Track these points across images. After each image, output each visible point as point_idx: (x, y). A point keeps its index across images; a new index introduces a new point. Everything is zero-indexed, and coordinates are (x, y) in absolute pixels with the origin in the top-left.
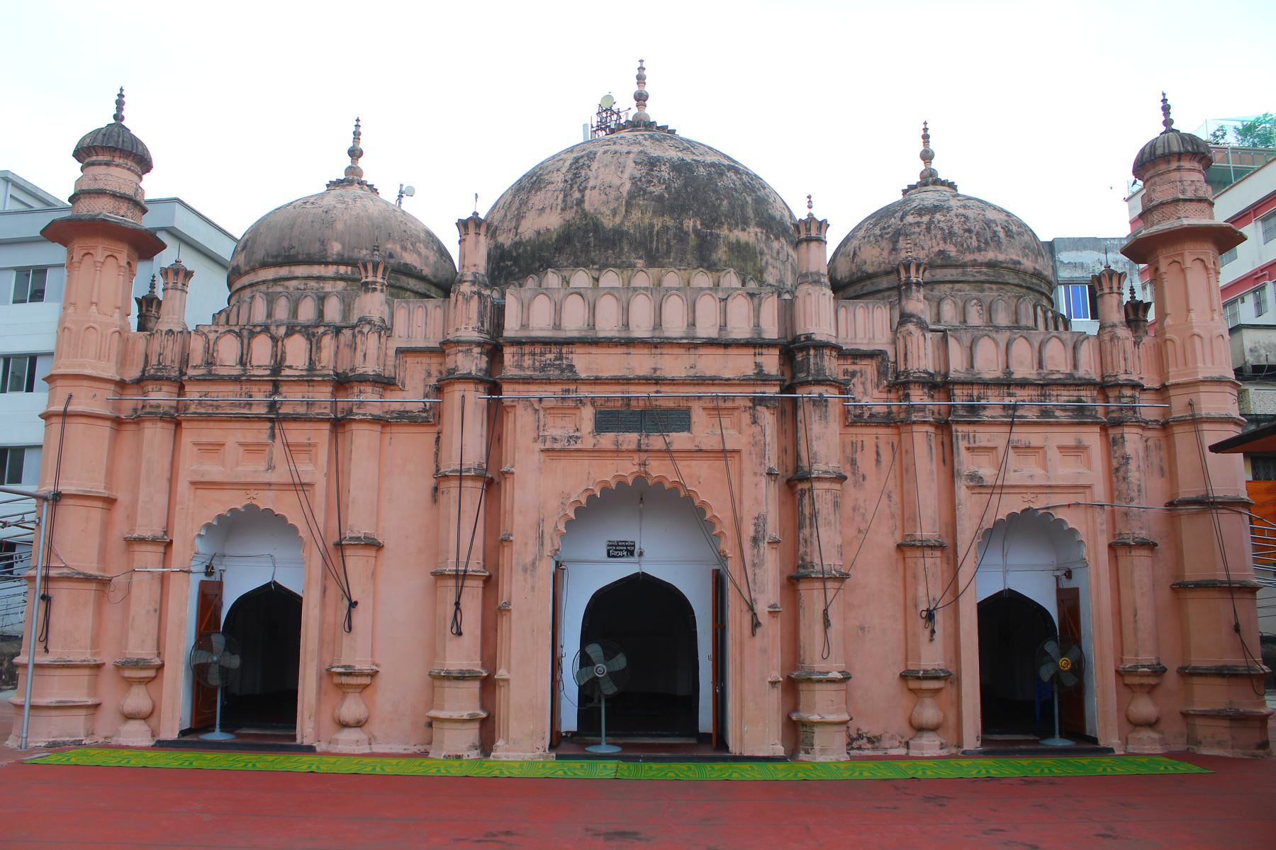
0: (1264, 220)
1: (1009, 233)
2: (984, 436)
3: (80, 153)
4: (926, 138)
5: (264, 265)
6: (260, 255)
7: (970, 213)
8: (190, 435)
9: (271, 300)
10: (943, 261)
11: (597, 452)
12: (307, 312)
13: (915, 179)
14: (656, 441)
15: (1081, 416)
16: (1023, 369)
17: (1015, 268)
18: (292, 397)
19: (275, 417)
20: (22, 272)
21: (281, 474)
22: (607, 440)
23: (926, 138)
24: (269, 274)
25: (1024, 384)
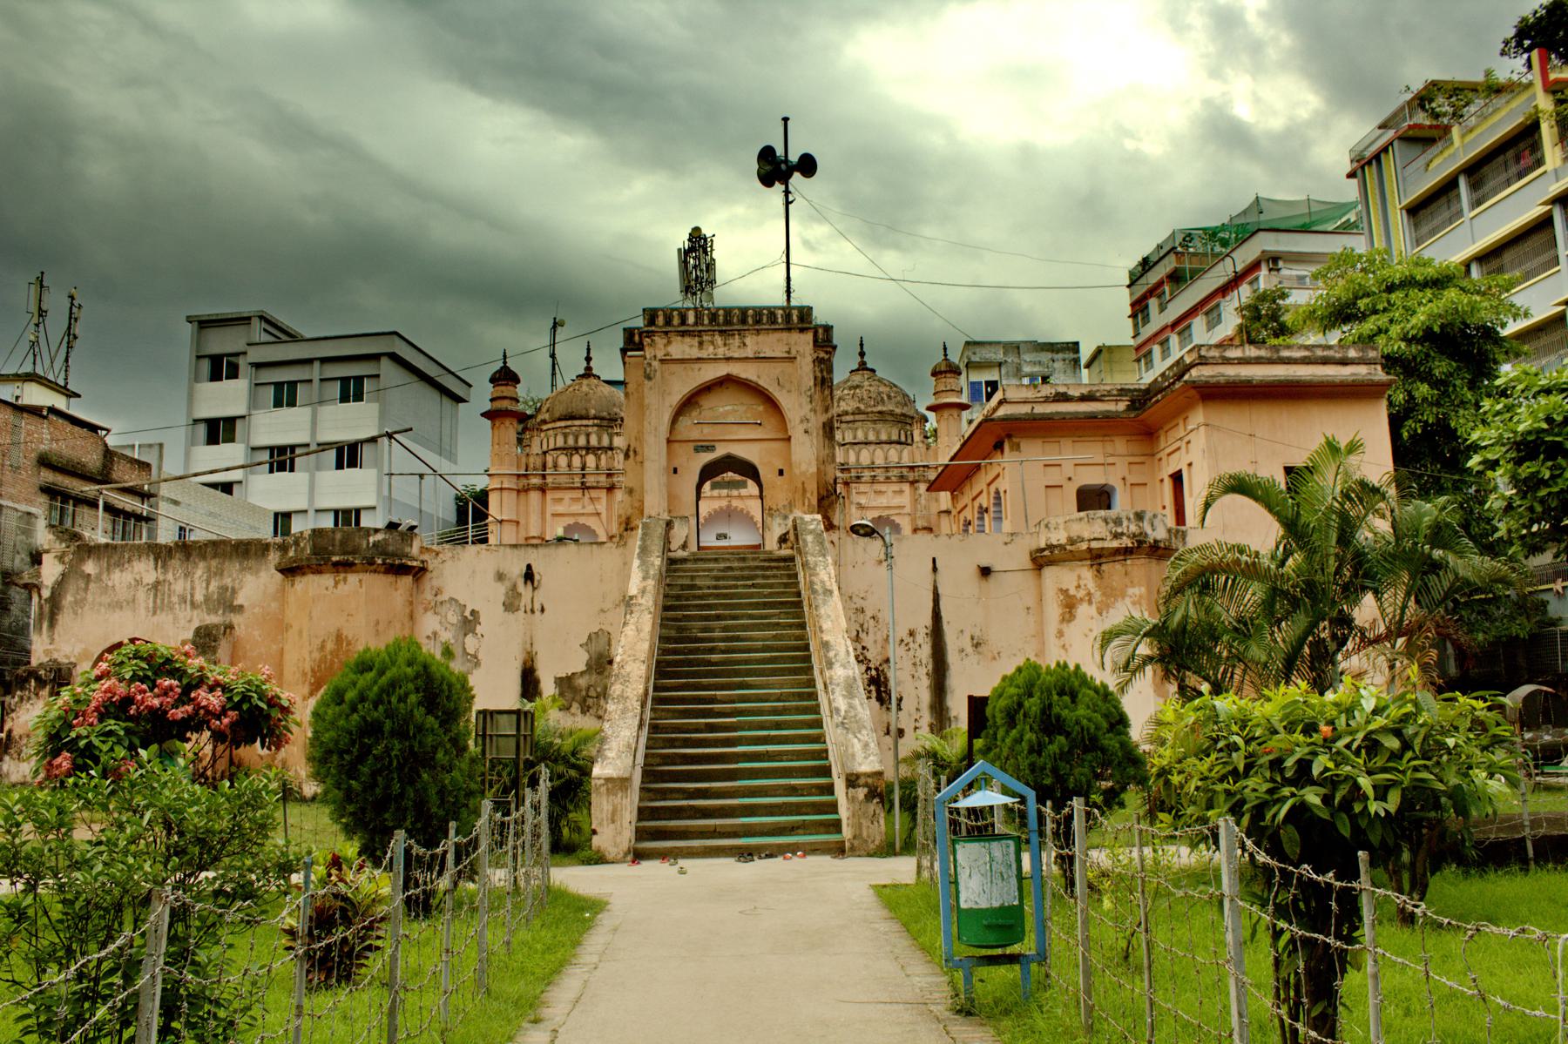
0: (1207, 314)
2: (862, 488)
3: (492, 380)
4: (862, 345)
5: (560, 419)
6: (557, 415)
8: (550, 495)
9: (565, 436)
10: (858, 412)
11: (712, 497)
12: (582, 441)
13: (856, 366)
14: (735, 493)
15: (902, 479)
16: (880, 461)
17: (891, 413)
18: (590, 480)
19: (584, 487)
20: (278, 386)
21: (590, 509)
22: (716, 493)
23: (862, 345)
24: (563, 424)
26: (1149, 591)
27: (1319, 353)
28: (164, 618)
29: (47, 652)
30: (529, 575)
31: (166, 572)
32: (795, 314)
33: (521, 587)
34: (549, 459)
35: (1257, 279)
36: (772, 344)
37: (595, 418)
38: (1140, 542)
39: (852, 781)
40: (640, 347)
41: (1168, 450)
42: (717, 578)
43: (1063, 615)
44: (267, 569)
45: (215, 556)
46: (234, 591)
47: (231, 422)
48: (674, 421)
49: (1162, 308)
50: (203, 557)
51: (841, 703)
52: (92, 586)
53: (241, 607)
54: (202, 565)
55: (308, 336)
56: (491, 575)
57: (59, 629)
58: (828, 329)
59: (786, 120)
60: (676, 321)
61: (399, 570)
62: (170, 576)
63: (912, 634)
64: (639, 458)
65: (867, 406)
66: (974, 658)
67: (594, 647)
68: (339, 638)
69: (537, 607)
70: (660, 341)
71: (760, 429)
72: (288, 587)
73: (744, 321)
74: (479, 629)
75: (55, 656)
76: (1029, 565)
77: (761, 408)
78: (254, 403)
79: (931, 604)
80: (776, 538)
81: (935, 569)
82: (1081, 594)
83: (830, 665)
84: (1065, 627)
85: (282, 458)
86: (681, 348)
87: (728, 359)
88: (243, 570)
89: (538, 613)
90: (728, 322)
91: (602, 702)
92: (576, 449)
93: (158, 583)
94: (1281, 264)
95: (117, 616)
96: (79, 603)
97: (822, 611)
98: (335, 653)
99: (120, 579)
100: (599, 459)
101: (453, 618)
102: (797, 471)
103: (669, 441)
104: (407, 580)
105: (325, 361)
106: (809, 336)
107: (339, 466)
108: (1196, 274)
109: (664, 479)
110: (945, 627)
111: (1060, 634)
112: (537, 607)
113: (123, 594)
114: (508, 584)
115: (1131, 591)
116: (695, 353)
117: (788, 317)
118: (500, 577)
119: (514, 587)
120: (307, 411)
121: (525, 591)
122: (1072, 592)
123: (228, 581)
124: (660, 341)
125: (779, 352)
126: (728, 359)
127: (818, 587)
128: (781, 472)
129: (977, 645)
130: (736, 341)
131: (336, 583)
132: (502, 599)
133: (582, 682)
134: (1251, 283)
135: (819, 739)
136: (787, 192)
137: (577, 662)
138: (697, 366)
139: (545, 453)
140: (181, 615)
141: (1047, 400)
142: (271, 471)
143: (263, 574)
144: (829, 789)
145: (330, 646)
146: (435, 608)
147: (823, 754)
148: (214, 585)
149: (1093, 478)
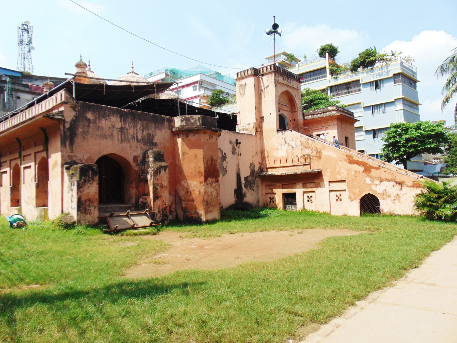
28: (125, 144)
31: (125, 124)
35: (196, 86)
44: (164, 129)
45: (145, 120)
46: (153, 137)
50: (140, 120)
53: (156, 143)
54: (140, 123)
56: (228, 142)
57: (75, 145)
59: (274, 17)
62: (127, 126)
68: (212, 159)
69: (239, 154)
75: (74, 159)
88: (155, 128)
93: (122, 130)
95: (104, 142)
96: (85, 133)
98: (211, 165)
99: (105, 123)
112: (239, 154)
113: (107, 132)
118: (231, 142)
119: (234, 147)
123: (150, 131)
126: (288, 86)
132: (231, 150)
134: (194, 87)
140: (133, 144)
145: (209, 162)
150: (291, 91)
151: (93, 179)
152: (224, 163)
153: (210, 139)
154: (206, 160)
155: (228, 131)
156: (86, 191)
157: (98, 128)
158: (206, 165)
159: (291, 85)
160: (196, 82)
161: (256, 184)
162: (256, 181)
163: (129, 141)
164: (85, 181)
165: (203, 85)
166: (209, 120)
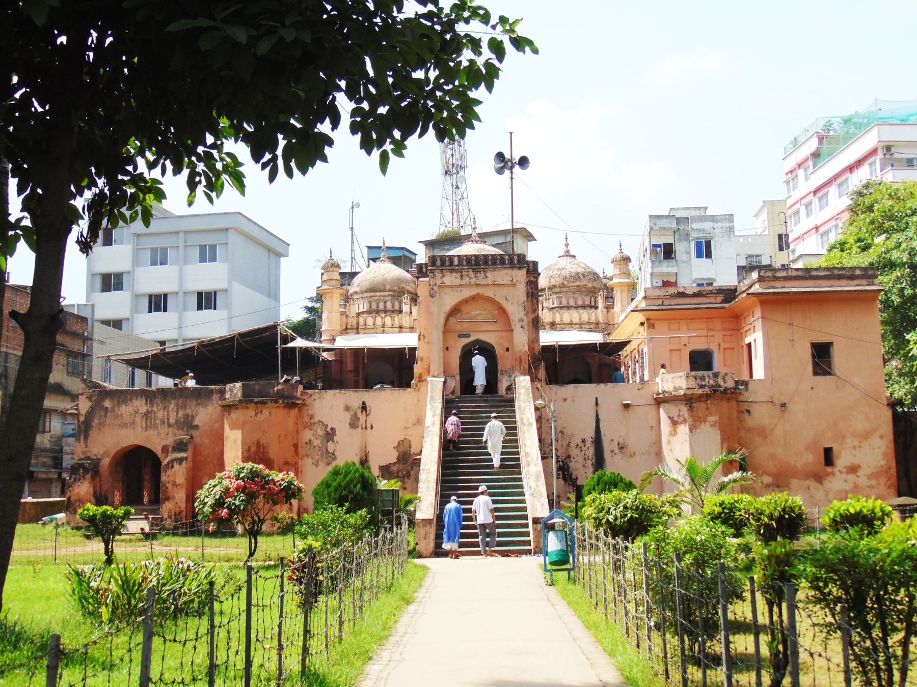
1: (584, 275)
5: (366, 292)
6: (364, 289)
7: (572, 270)
9: (370, 303)
12: (381, 306)
13: (562, 253)
16: (576, 320)
24: (369, 294)
25: (575, 324)
26: (721, 418)
27: (836, 272)
28: (151, 432)
29: (83, 452)
30: (364, 408)
32: (516, 257)
33: (359, 414)
34: (361, 320)
35: (875, 162)
36: (502, 276)
37: (390, 291)
38: (715, 391)
39: (536, 521)
40: (425, 276)
41: (746, 329)
42: (472, 412)
43: (670, 432)
44: (212, 405)
45: (181, 397)
46: (193, 417)
47: (119, 276)
48: (447, 320)
49: (807, 179)
50: (174, 398)
51: (533, 485)
52: (109, 414)
53: (197, 426)
54: (173, 402)
55: (178, 214)
56: (342, 407)
57: (90, 439)
58: (535, 264)
59: (511, 133)
60: (447, 263)
61: (293, 405)
62: (155, 409)
63: (583, 441)
64: (426, 340)
65: (569, 282)
66: (619, 456)
67: (401, 449)
68: (258, 445)
69: (369, 426)
70: (438, 275)
71: (496, 325)
72: (226, 414)
73: (486, 263)
74: (335, 439)
75: (89, 454)
76: (653, 402)
77: (496, 312)
78: (136, 262)
79: (594, 424)
80: (504, 389)
81: (597, 404)
82: (681, 419)
83: (528, 465)
84: (671, 438)
85: (158, 303)
86: (450, 279)
87: (477, 285)
88: (198, 405)
89: (369, 429)
90: (477, 264)
91: (406, 480)
92: (378, 312)
93: (147, 414)
94: (893, 150)
97: (526, 435)
100: (393, 320)
101: (321, 432)
102: (517, 350)
103: (443, 332)
104: (294, 412)
105: (186, 232)
106: (524, 271)
107: (200, 308)
108: (831, 155)
109: (441, 354)
110: (603, 438)
111: (669, 442)
113: (127, 419)
114: (352, 412)
115: (709, 419)
116: (458, 282)
117: (511, 261)
118: (347, 408)
119: (355, 414)
120: (176, 268)
121: (362, 416)
122: (676, 419)
123: (189, 411)
124: (438, 275)
125: (505, 282)
126: (477, 285)
127: (525, 421)
128: (508, 349)
129: (621, 448)
130: (482, 275)
131: (256, 414)
133: (395, 468)
135: (523, 501)
136: (512, 178)
137: (391, 457)
138: (459, 289)
139: (358, 315)
140: (162, 431)
141: (672, 296)
142: (150, 311)
143: (210, 407)
144: (526, 526)
145: (253, 449)
146: (309, 426)
147: (525, 509)
148: (181, 414)
149: (700, 345)
150: (489, 293)
151: (84, 477)
152: (330, 444)
153: (256, 415)
154: (247, 447)
155: (343, 391)
156: (77, 491)
157: (117, 416)
158: (246, 454)
159: (489, 281)
160: (874, 152)
161: (412, 478)
162: (412, 473)
163: (156, 428)
164: (75, 480)
165: (896, 156)
166: (257, 387)
